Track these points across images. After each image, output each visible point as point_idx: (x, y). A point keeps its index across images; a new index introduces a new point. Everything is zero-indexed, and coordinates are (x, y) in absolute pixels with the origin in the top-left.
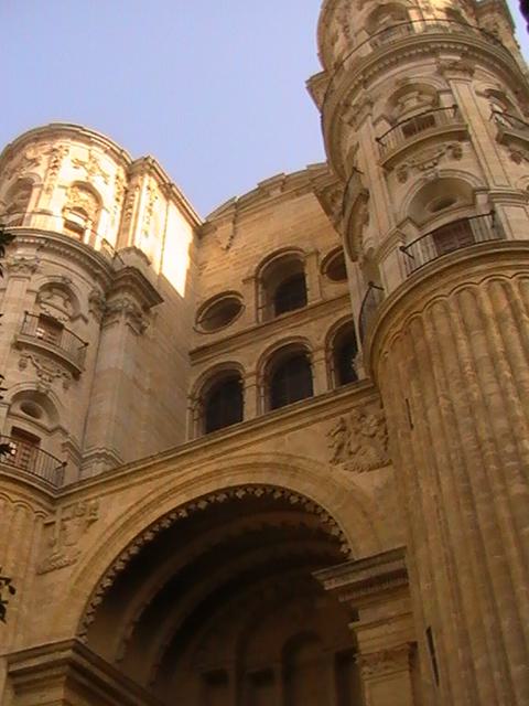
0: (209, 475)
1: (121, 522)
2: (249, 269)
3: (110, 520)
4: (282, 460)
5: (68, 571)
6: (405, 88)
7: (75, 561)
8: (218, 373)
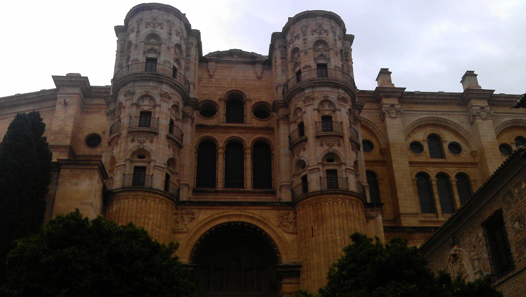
1: (204, 222)
4: (262, 219)
5: (185, 235)
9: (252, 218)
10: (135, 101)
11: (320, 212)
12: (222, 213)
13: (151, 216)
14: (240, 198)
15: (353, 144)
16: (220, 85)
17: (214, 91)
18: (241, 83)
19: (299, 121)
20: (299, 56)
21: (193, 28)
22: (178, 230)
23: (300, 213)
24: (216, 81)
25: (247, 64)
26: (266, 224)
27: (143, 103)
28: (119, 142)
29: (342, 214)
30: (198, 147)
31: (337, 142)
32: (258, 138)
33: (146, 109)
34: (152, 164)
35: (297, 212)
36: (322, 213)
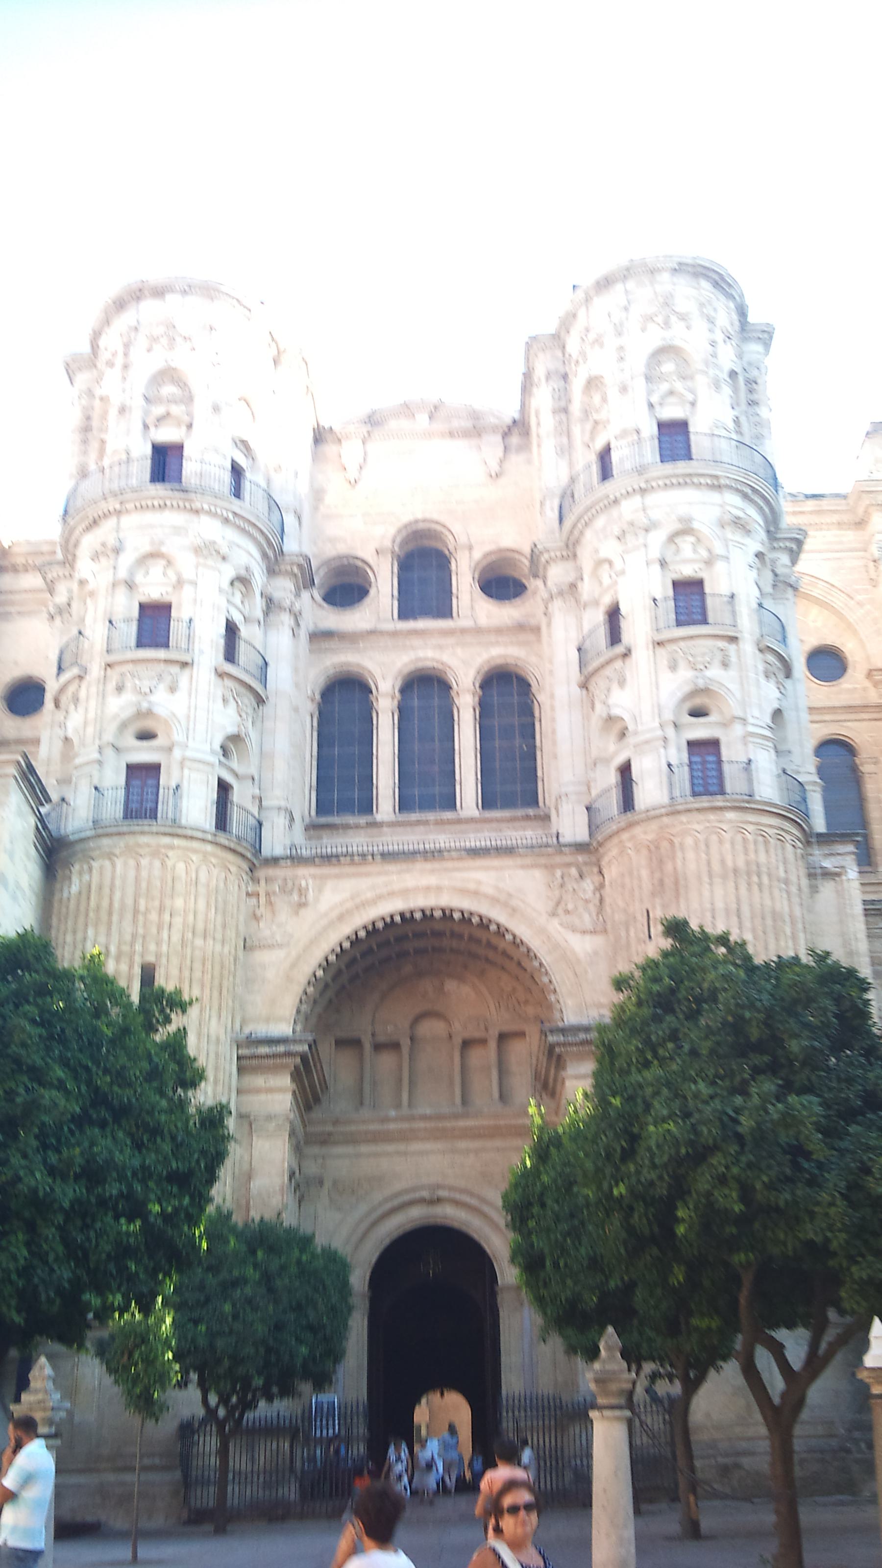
6: (686, 530)
9: (476, 893)
11: (669, 867)
14: (442, 839)
15: (771, 658)
19: (607, 601)
20: (604, 400)
23: (612, 872)
26: (514, 910)
28: (83, 694)
29: (736, 871)
31: (719, 656)
34: (177, 753)
35: (605, 871)
36: (675, 868)
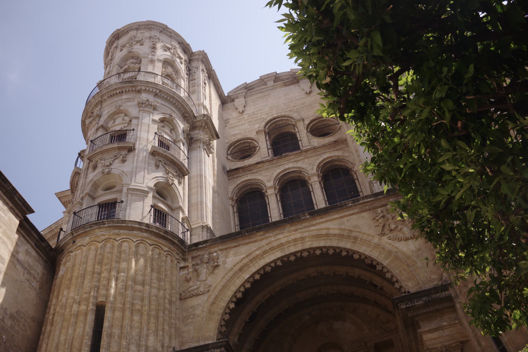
0: (295, 240)
2: (260, 126)
3: (229, 266)
4: (346, 233)
5: (204, 298)
7: (208, 291)
8: (246, 186)
9: (327, 235)
10: (100, 124)
12: (268, 244)
13: (123, 265)
16: (255, 119)
17: (249, 127)
18: (284, 107)
21: (194, 49)
22: (189, 292)
24: (249, 116)
25: (288, 85)
27: (113, 123)
30: (235, 198)
32: (325, 159)
33: (118, 128)
34: (125, 190)
